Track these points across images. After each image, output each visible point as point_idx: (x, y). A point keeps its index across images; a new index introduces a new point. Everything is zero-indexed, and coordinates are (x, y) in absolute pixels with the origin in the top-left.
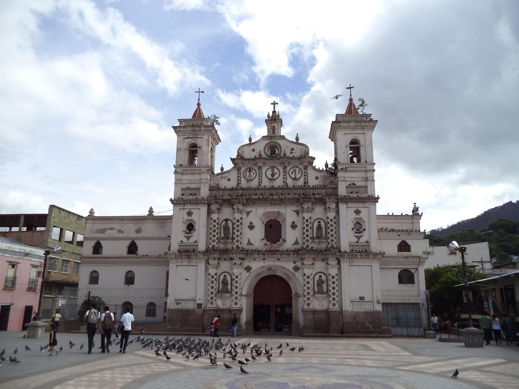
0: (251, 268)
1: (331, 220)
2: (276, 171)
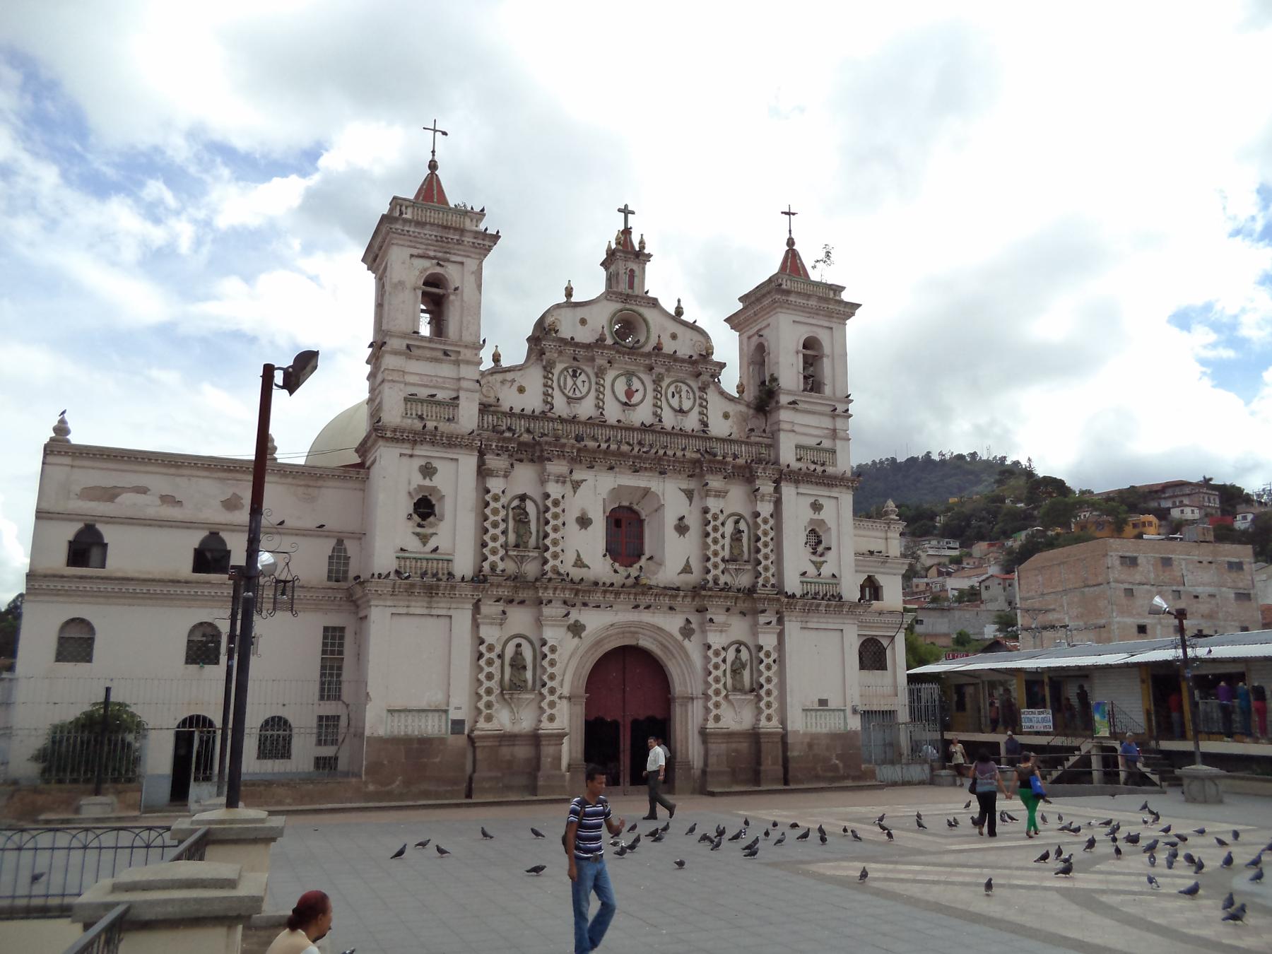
0: (583, 627)
2: (636, 384)
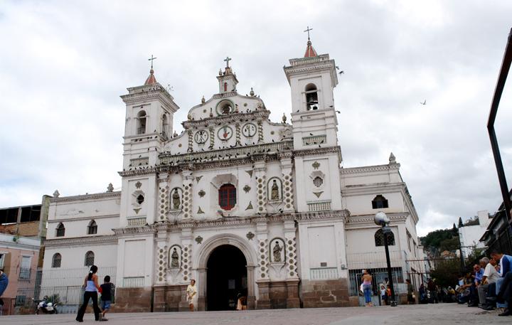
1: (287, 178)
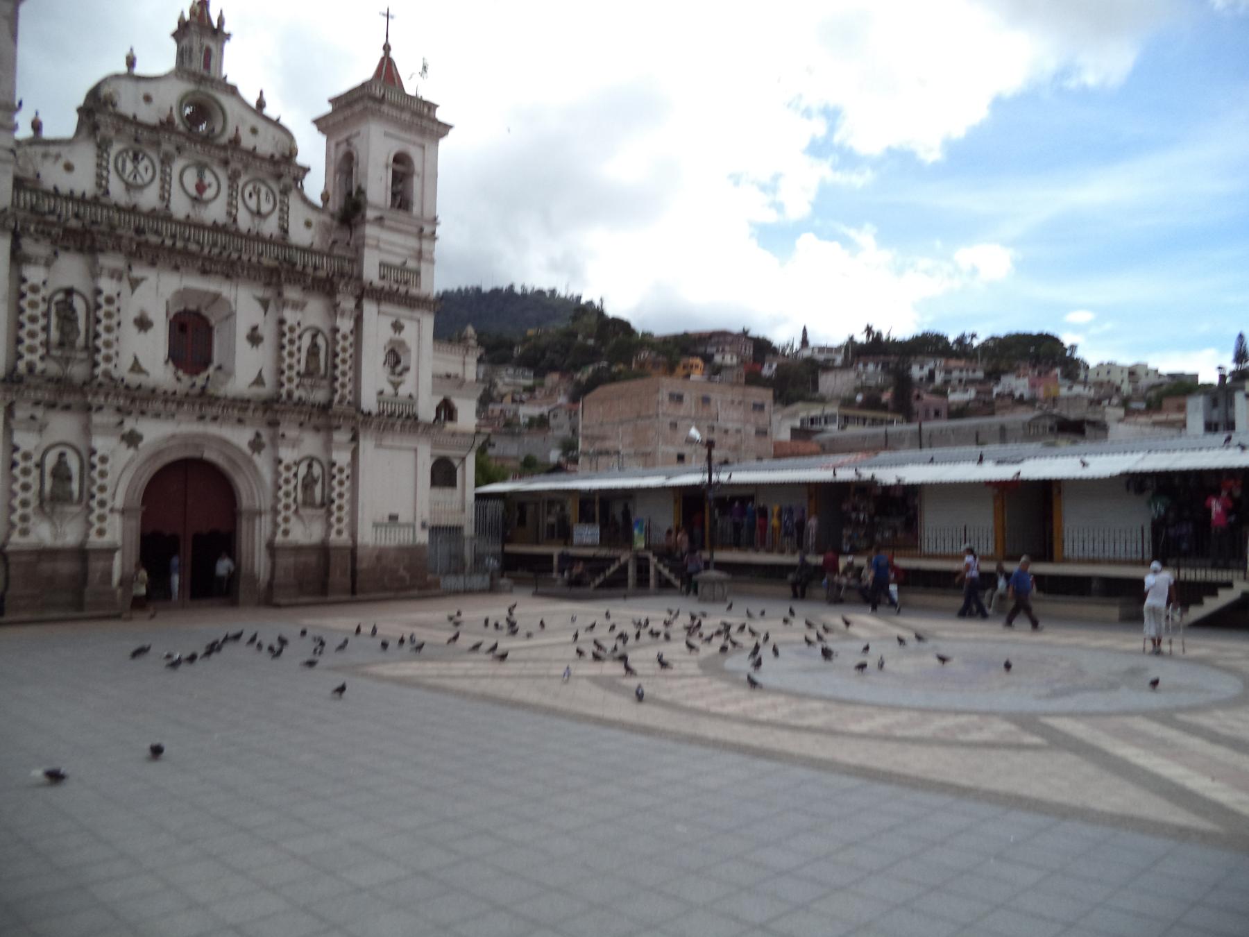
1: (345, 337)
2: (209, 178)
